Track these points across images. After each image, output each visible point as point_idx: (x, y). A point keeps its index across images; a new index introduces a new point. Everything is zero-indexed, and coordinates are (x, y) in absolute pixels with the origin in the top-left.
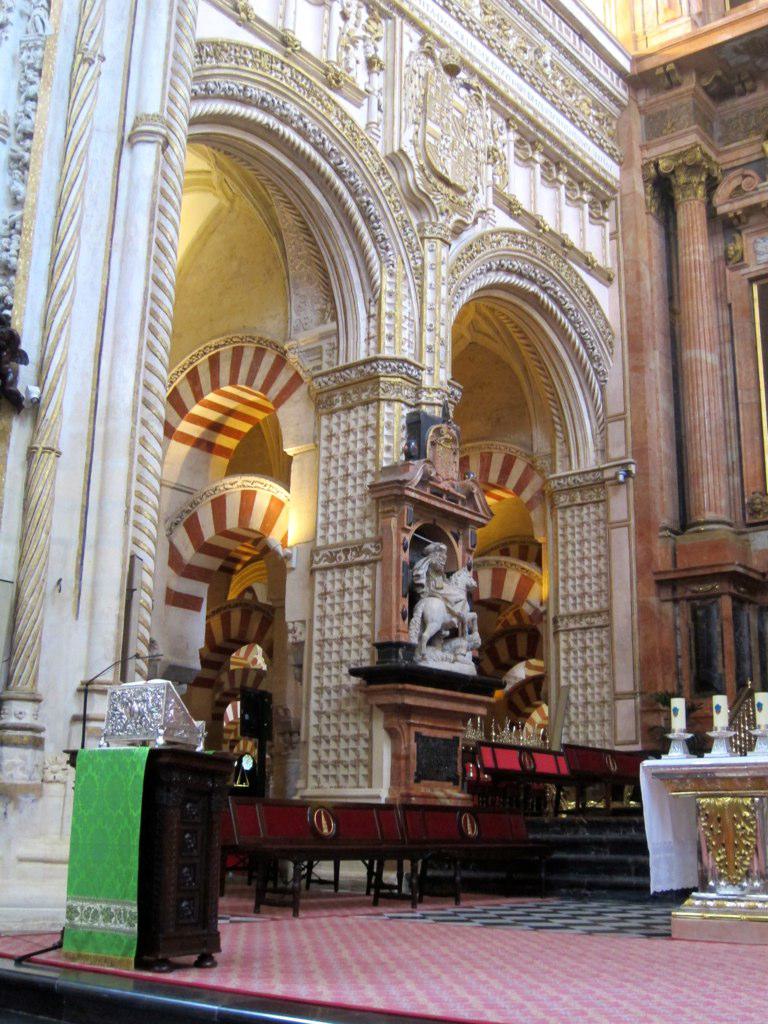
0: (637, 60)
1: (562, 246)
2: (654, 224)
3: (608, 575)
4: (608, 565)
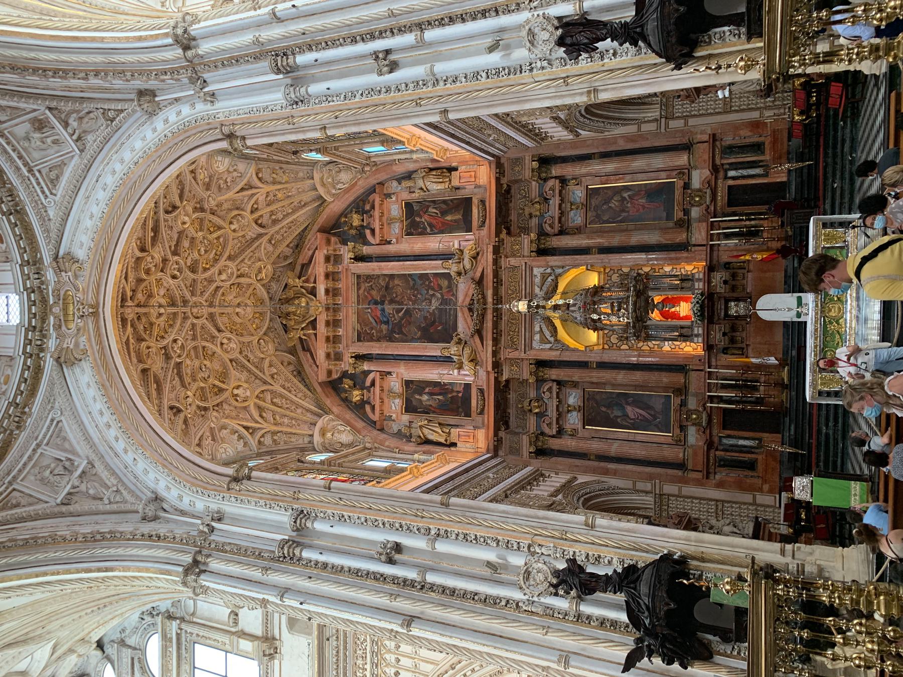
0: (488, 452)
1: (565, 488)
2: (554, 459)
3: (701, 499)
4: (696, 498)
